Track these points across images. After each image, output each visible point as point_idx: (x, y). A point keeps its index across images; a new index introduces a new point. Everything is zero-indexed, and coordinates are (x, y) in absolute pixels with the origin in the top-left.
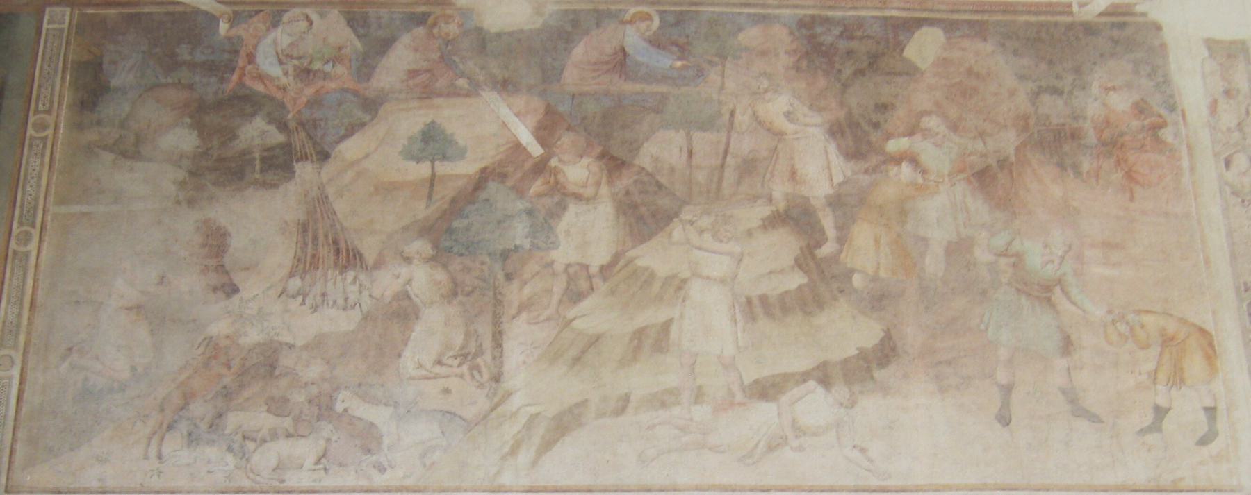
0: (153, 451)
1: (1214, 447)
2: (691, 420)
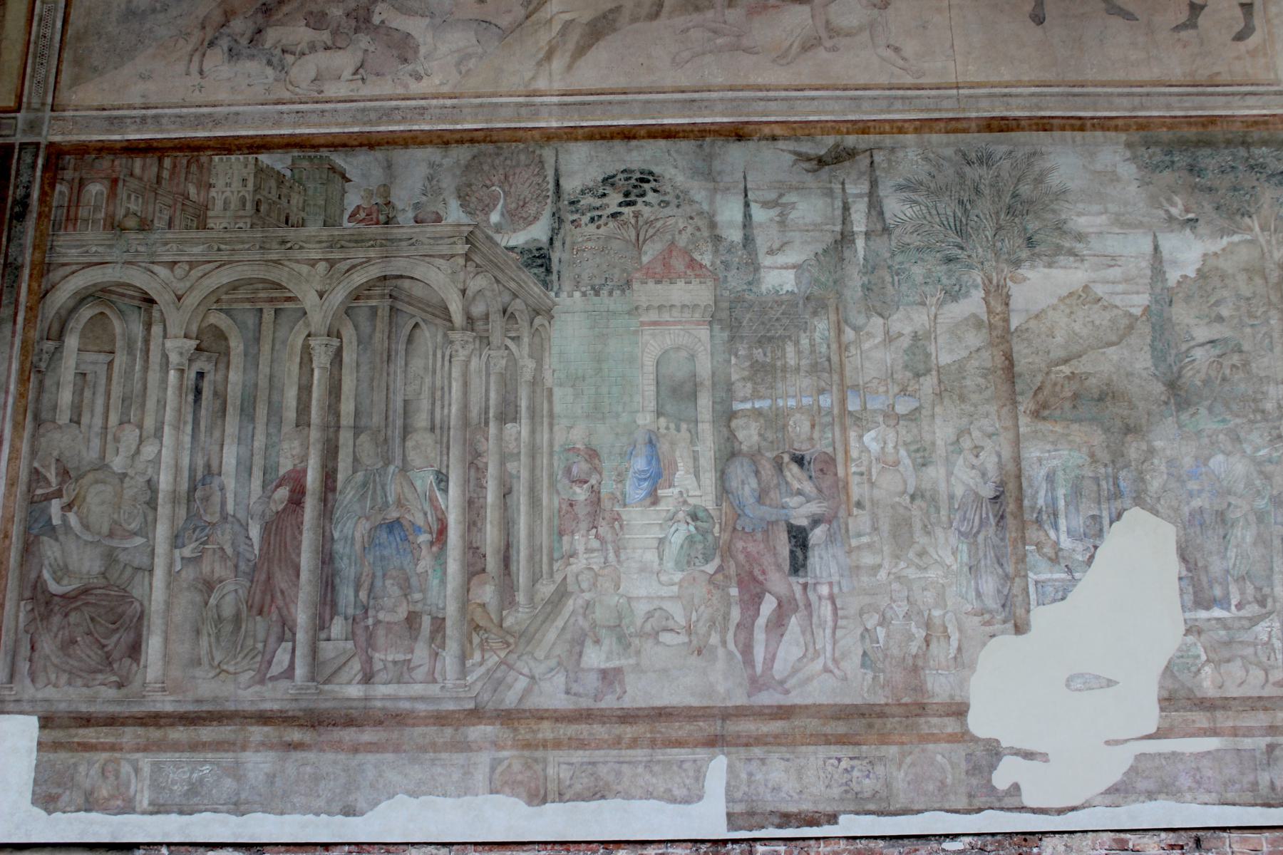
0: (194, 67)
1: (1253, 41)
2: (725, 22)
